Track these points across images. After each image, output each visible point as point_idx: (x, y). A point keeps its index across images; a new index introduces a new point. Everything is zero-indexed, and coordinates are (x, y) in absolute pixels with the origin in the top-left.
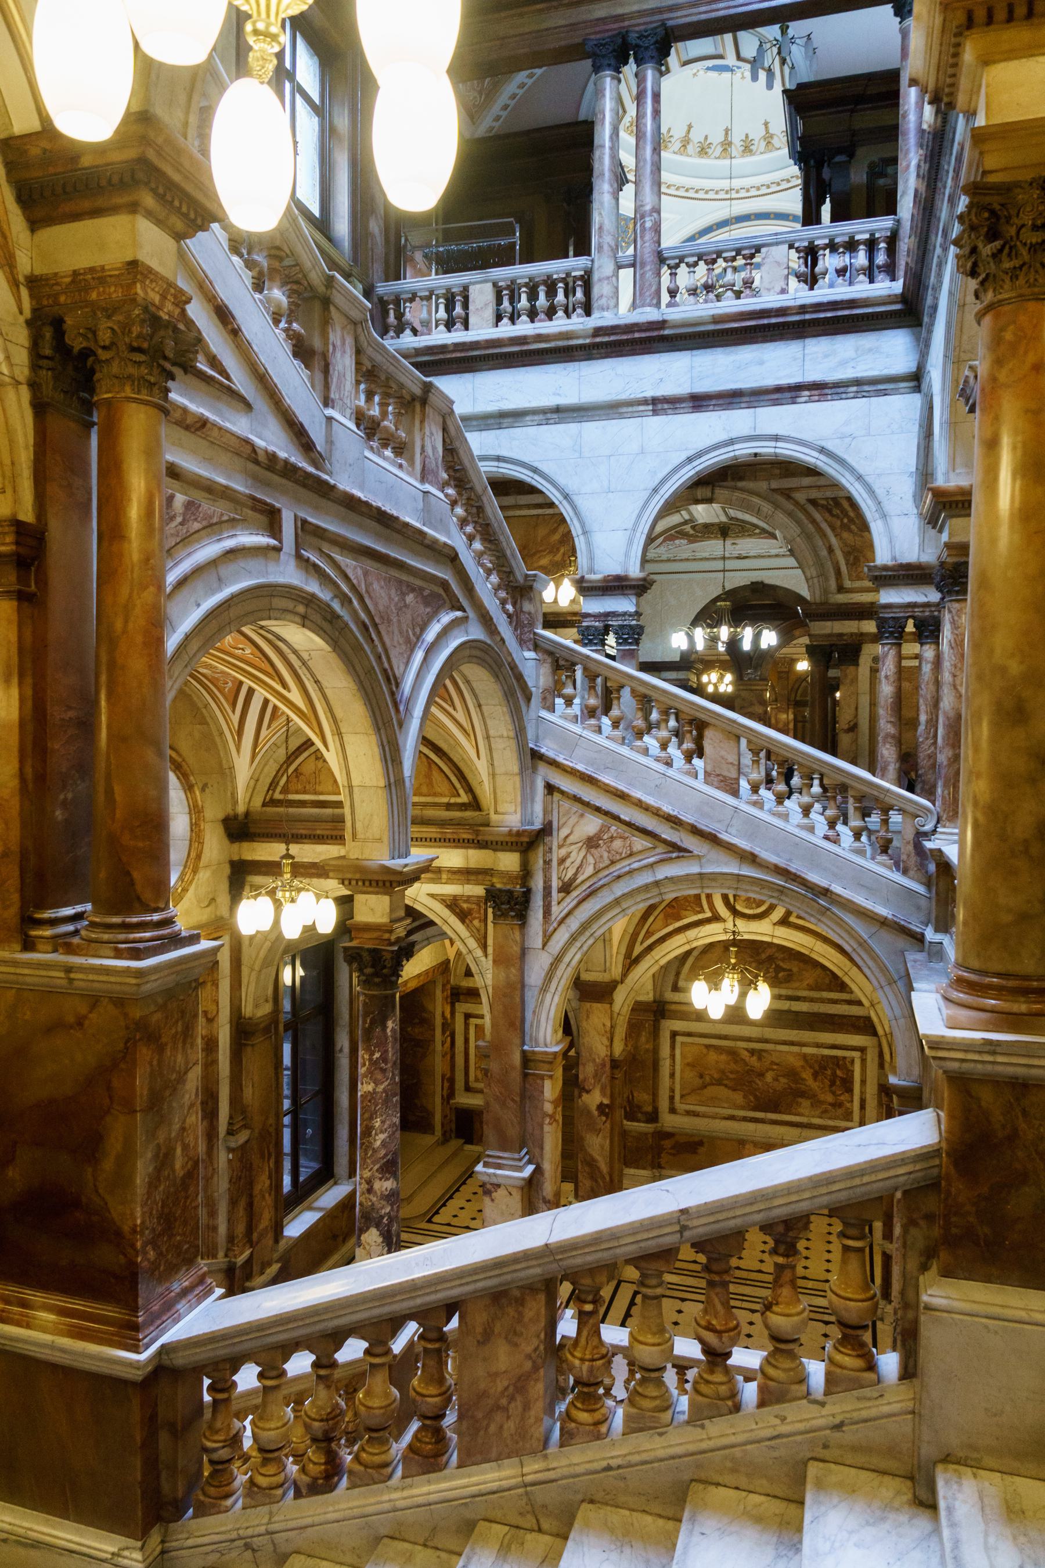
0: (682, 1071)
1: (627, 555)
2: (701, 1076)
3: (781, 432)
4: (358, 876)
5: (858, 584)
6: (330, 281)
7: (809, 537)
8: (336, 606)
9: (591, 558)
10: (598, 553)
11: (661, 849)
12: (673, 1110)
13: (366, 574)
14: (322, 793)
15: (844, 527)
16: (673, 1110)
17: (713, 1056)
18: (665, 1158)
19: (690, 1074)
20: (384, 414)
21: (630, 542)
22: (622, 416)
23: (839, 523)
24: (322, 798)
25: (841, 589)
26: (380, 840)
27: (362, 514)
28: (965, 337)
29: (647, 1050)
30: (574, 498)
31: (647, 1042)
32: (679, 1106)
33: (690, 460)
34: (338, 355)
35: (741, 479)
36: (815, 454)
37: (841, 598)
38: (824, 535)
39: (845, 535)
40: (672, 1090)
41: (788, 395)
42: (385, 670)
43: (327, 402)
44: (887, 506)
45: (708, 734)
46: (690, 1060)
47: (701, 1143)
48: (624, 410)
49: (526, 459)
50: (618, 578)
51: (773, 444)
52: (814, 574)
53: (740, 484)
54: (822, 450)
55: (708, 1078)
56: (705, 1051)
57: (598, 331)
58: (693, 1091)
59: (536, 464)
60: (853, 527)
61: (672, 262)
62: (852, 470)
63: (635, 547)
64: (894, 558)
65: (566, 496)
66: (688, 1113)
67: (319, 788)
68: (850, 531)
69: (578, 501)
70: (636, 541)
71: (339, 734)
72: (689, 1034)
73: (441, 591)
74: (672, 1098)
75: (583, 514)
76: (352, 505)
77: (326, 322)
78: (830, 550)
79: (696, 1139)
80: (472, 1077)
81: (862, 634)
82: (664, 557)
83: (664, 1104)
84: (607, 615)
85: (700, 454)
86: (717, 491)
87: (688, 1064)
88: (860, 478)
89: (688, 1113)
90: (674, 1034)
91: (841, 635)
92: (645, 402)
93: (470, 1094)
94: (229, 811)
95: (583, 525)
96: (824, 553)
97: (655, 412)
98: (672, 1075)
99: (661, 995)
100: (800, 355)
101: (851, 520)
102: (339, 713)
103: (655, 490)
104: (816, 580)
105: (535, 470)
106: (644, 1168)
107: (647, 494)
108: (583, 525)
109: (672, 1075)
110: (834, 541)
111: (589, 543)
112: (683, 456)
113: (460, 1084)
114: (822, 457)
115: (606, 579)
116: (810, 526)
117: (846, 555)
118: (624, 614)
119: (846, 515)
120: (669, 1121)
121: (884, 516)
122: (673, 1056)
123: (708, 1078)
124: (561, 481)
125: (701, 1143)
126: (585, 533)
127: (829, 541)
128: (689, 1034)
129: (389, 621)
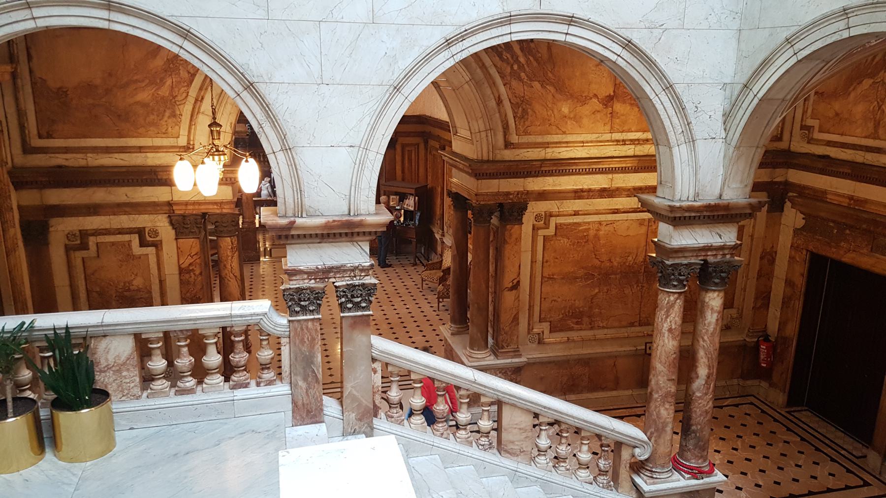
3: (579, 14)
5: (525, 139)
7: (478, 85)
15: (515, 75)
21: (360, 165)
23: (509, 70)
25: (508, 145)
30: (261, 88)
33: (449, 43)
36: (618, 49)
37: (509, 155)
38: (493, 84)
39: (514, 83)
44: (699, 131)
49: (164, 13)
51: (564, 28)
52: (482, 128)
54: (628, 45)
59: (187, 23)
60: (523, 74)
62: (661, 76)
63: (367, 172)
64: (697, 195)
65: (250, 87)
68: (520, 79)
69: (271, 94)
70: (368, 164)
75: (281, 122)
78: (499, 102)
81: (528, 193)
85: (463, 36)
88: (669, 88)
91: (508, 194)
96: (493, 103)
101: (521, 67)
104: (483, 134)
105: (186, 34)
110: (502, 89)
111: (293, 166)
112: (437, 37)
114: (625, 54)
115: (327, 226)
116: (479, 70)
117: (515, 106)
119: (517, 61)
121: (692, 141)
124: (237, 57)
127: (498, 90)
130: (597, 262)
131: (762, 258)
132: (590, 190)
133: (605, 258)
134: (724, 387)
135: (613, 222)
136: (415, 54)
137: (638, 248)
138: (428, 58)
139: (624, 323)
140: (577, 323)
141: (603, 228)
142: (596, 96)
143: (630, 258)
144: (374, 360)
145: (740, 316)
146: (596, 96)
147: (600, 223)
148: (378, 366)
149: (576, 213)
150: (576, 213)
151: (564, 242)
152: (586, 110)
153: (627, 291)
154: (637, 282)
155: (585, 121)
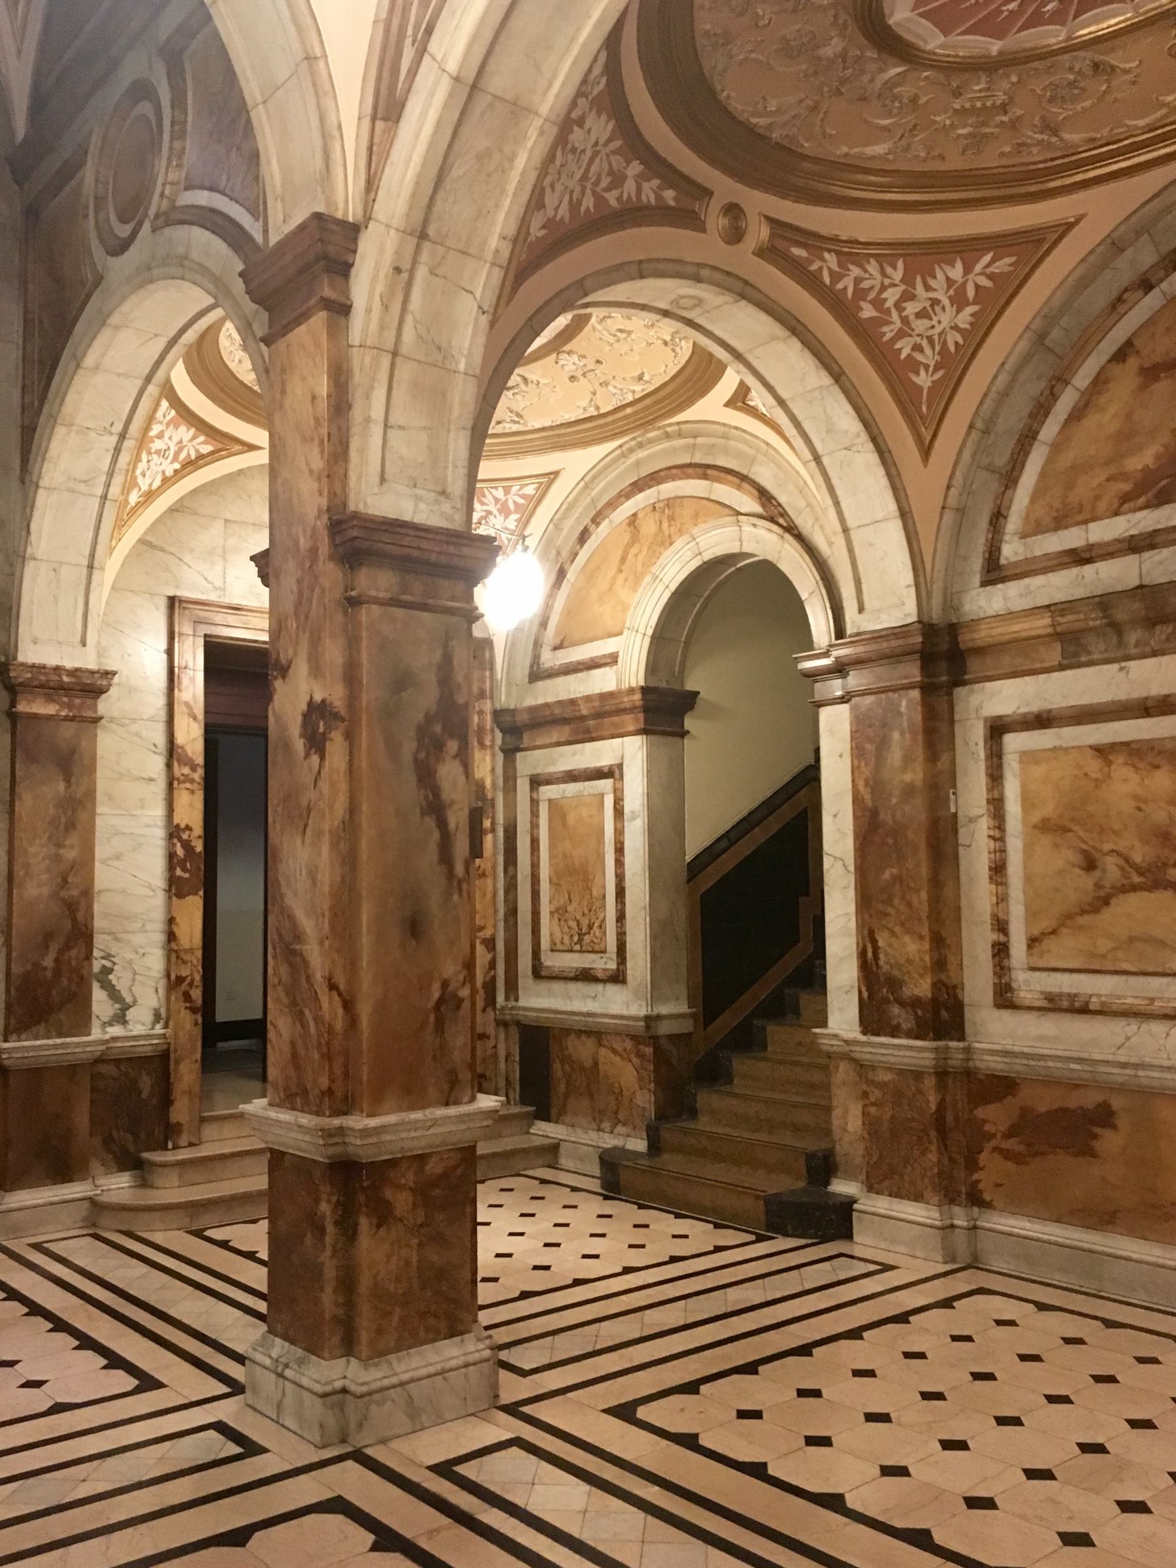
0: (1028, 851)
2: (1090, 865)
12: (1005, 998)
16: (1005, 998)
17: (1125, 782)
18: (992, 1170)
19: (1058, 859)
29: (909, 791)
31: (907, 759)
32: (1030, 985)
40: (1001, 926)
46: (1048, 810)
47: (1104, 1116)
55: (1111, 869)
56: (1094, 766)
58: (1066, 919)
66: (1054, 1005)
72: (1041, 721)
74: (1001, 951)
79: (1090, 1099)
80: (545, 944)
83: (977, 982)
87: (1044, 826)
89: (1054, 1005)
90: (997, 729)
93: (544, 986)
98: (998, 870)
99: (951, 602)
106: (918, 1198)
109: (998, 870)
113: (525, 962)
120: (998, 1036)
122: (997, 806)
123: (1111, 869)
125: (1104, 1116)
128: (1041, 721)
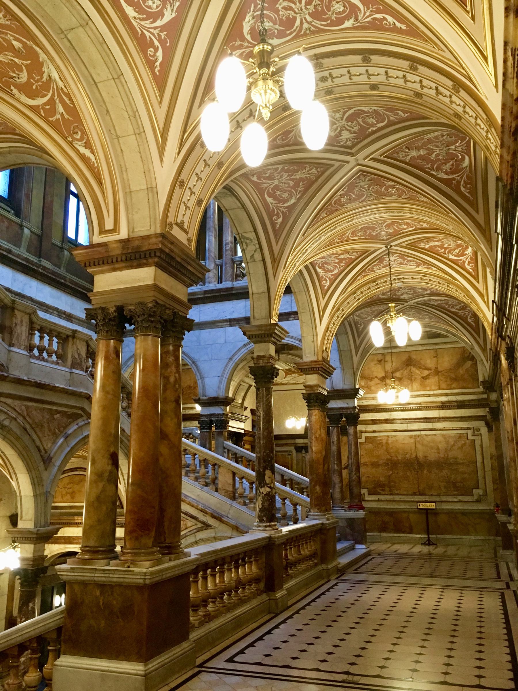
1: (219, 387)
4: (20, 536)
6: (14, 301)
8: (6, 423)
9: (204, 390)
10: (207, 387)
11: (199, 525)
13: (27, 407)
14: (56, 502)
20: (50, 344)
21: (220, 382)
22: (217, 327)
24: (56, 504)
26: (31, 520)
27: (26, 385)
28: (300, 304)
30: (198, 363)
34: (18, 327)
35: (291, 350)
36: (298, 342)
41: (285, 317)
42: (38, 447)
43: (11, 345)
45: (221, 470)
48: (218, 324)
50: (214, 398)
53: (291, 352)
57: (206, 292)
61: (238, 263)
65: (194, 362)
67: (55, 500)
69: (199, 364)
71: (15, 474)
73: (81, 412)
76: (19, 382)
77: (13, 315)
82: (292, 382)
84: (211, 415)
86: (280, 355)
92: (226, 321)
94: (13, 512)
95: (200, 375)
97: (231, 325)
100: (290, 300)
102: (14, 466)
103: (231, 359)
107: (227, 361)
108: (200, 375)
111: (203, 383)
118: (218, 414)
126: (201, 378)
129: (42, 426)
130: (389, 457)
131: (491, 458)
132: (379, 420)
133: (393, 455)
134: (483, 540)
135: (394, 436)
136: (236, 350)
137: (411, 450)
138: (239, 350)
139: (410, 493)
140: (383, 490)
141: (390, 439)
142: (376, 377)
143: (407, 456)
144: (225, 448)
145: (486, 494)
146: (376, 377)
147: (388, 436)
148: (226, 450)
149: (374, 431)
150: (374, 431)
151: (370, 446)
152: (372, 383)
153: (408, 474)
154: (414, 469)
155: (373, 388)
